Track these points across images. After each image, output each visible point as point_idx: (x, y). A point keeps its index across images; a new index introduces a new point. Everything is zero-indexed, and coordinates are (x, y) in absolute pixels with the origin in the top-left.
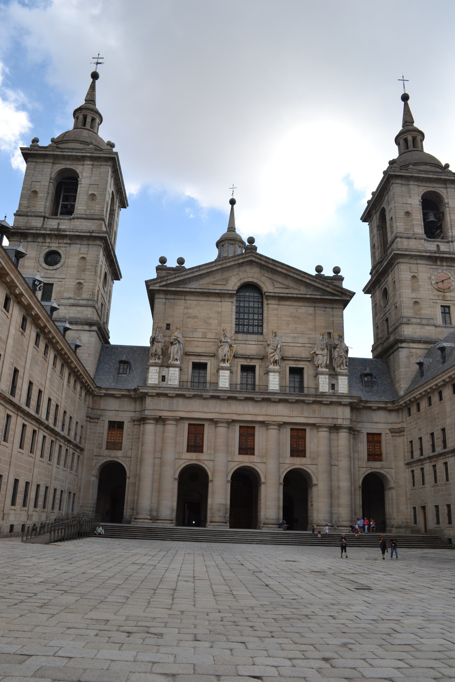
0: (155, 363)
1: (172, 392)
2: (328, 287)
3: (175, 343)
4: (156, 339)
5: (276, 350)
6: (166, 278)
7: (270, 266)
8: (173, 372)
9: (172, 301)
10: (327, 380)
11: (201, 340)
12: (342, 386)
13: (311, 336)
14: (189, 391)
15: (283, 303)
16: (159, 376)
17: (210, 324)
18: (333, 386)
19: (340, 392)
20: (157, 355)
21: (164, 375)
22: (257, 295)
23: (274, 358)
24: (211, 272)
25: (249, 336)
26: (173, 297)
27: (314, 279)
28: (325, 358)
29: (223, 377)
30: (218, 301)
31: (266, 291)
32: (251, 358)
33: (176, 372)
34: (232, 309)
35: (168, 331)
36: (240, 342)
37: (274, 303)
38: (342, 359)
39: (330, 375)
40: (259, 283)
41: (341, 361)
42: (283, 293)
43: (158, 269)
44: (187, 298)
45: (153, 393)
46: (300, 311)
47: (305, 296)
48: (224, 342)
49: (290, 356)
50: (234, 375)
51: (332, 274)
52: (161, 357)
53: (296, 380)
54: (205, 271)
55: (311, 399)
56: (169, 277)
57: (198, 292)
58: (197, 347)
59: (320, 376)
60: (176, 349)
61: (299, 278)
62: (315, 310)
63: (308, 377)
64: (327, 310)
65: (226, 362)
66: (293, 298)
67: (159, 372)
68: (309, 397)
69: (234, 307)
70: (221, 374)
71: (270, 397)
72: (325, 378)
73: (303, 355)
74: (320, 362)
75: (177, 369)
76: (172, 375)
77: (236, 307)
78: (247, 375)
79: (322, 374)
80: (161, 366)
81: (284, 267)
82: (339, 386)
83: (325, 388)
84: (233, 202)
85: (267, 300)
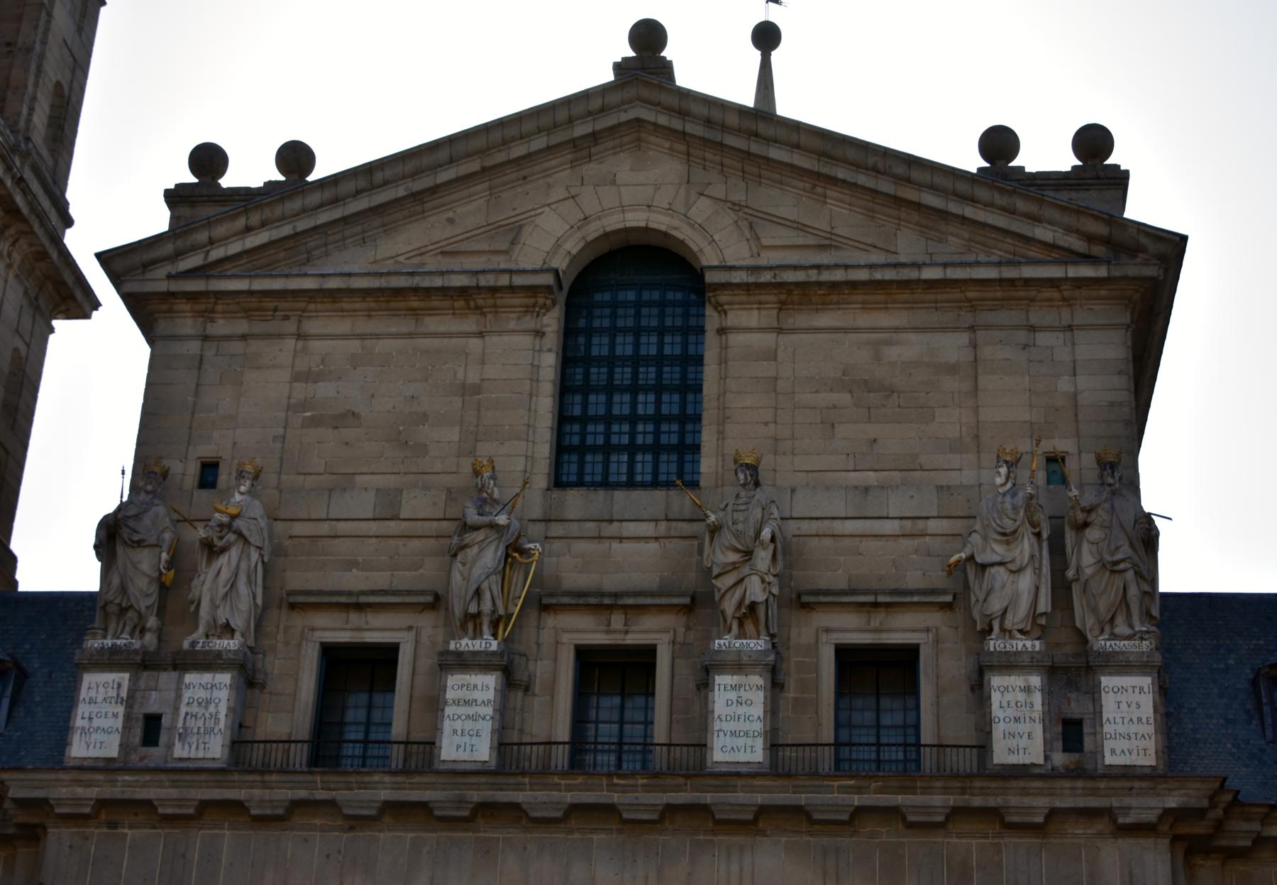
0: (115, 650)
1: (173, 793)
2: (1036, 219)
3: (220, 544)
4: (125, 533)
5: (748, 554)
6: (202, 236)
7: (730, 140)
8: (203, 694)
9: (236, 347)
10: (1037, 698)
11: (374, 527)
12: (1121, 729)
13: (953, 478)
14: (265, 785)
15: (801, 319)
16: (128, 717)
17: (422, 449)
18: (1071, 732)
19: (1109, 760)
20: (130, 614)
21: (153, 708)
22: (679, 296)
23: (738, 593)
24: (434, 190)
25: (619, 495)
26: (242, 327)
27: (962, 187)
28: (1025, 582)
29: (462, 710)
30: (467, 335)
32: (625, 608)
33: (216, 694)
34: (535, 367)
35: (205, 493)
36: (574, 529)
37: (754, 324)
38: (1118, 582)
40: (683, 233)
41: (1112, 596)
42: (796, 268)
43: (175, 197)
44: (312, 326)
45: (77, 801)
46: (892, 353)
47: (913, 274)
48: (476, 528)
49: (843, 585)
50: (537, 703)
52: (152, 622)
53: (886, 720)
54: (401, 192)
55: (937, 800)
56: (220, 230)
57: (366, 293)
58: (351, 564)
59: (996, 681)
60: (225, 575)
61: (885, 186)
62: (974, 345)
63: (939, 692)
64: (1043, 339)
65: (486, 628)
66: (854, 285)
67: (131, 695)
68: (926, 791)
69: (550, 361)
70: (450, 695)
71: (708, 798)
72: (1027, 690)
73: (913, 579)
74: (996, 606)
75: (225, 678)
76: (195, 709)
77: (567, 361)
78: (622, 708)
79: (1010, 664)
80: (144, 664)
81: (804, 139)
82: (1107, 728)
83: (1024, 742)
84: (766, 37)
85: (721, 309)
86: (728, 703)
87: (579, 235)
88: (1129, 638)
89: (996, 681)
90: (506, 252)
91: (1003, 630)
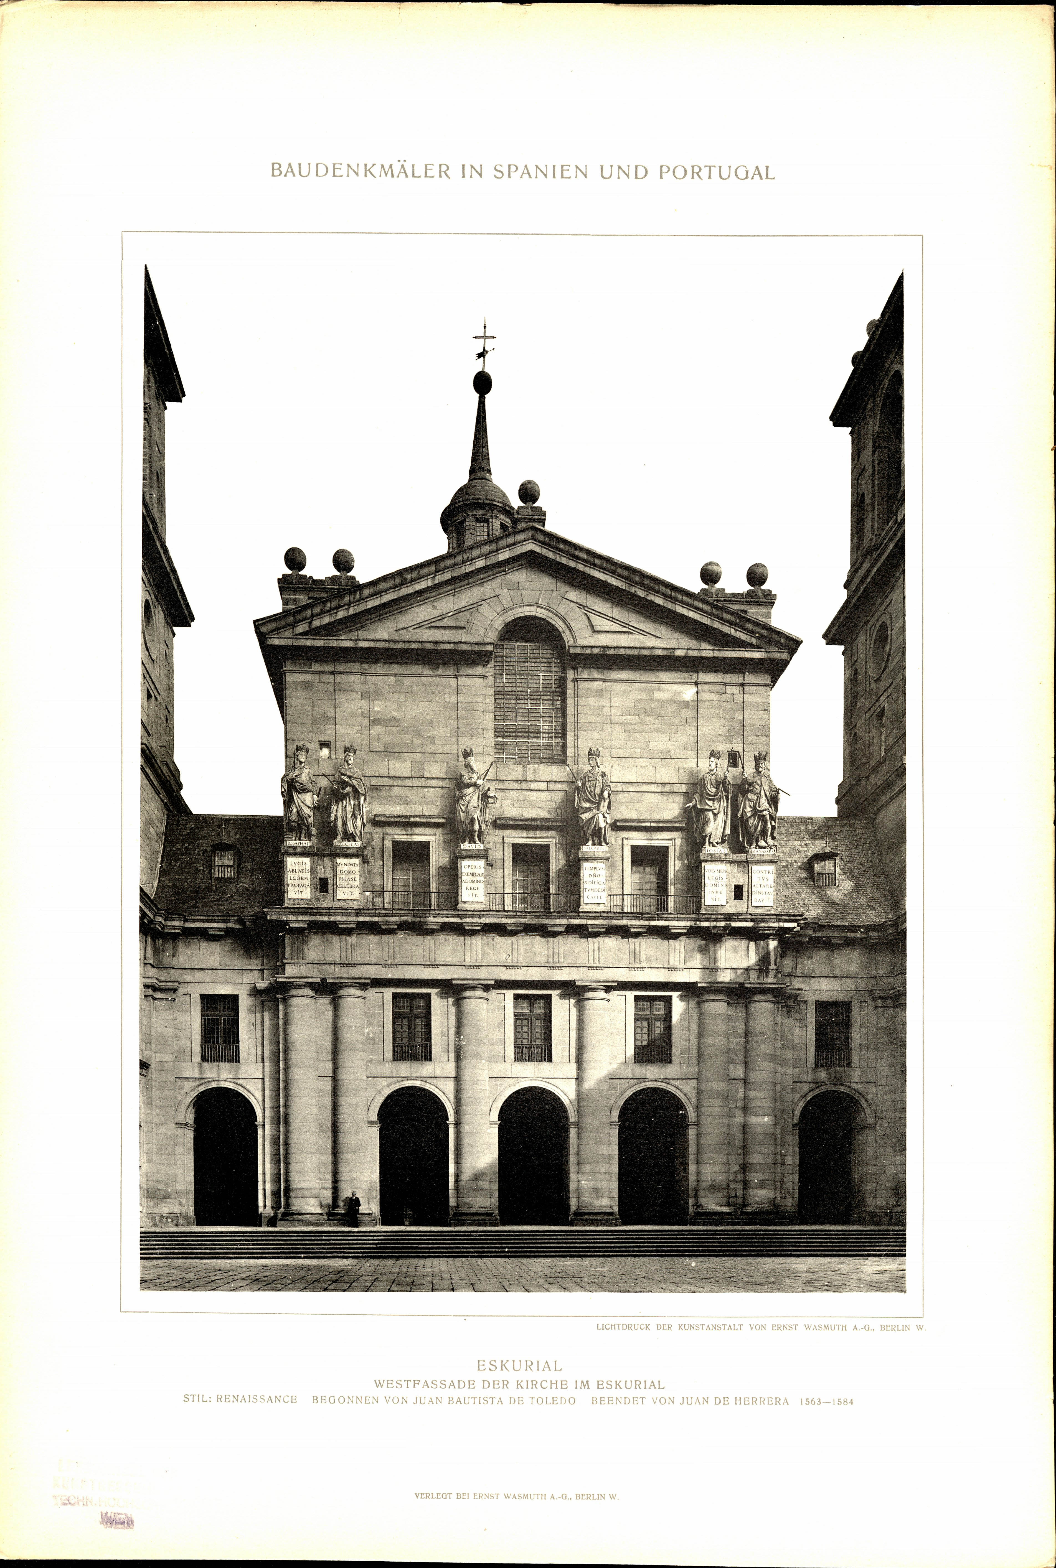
30: (449, 676)
31: (572, 643)
39: (731, 862)
51: (743, 587)
52: (314, 831)
70: (464, 870)
75: (356, 861)
79: (713, 859)
86: (590, 876)
87: (501, 619)
88: (764, 848)
89: (707, 867)
90: (464, 628)
91: (710, 843)
